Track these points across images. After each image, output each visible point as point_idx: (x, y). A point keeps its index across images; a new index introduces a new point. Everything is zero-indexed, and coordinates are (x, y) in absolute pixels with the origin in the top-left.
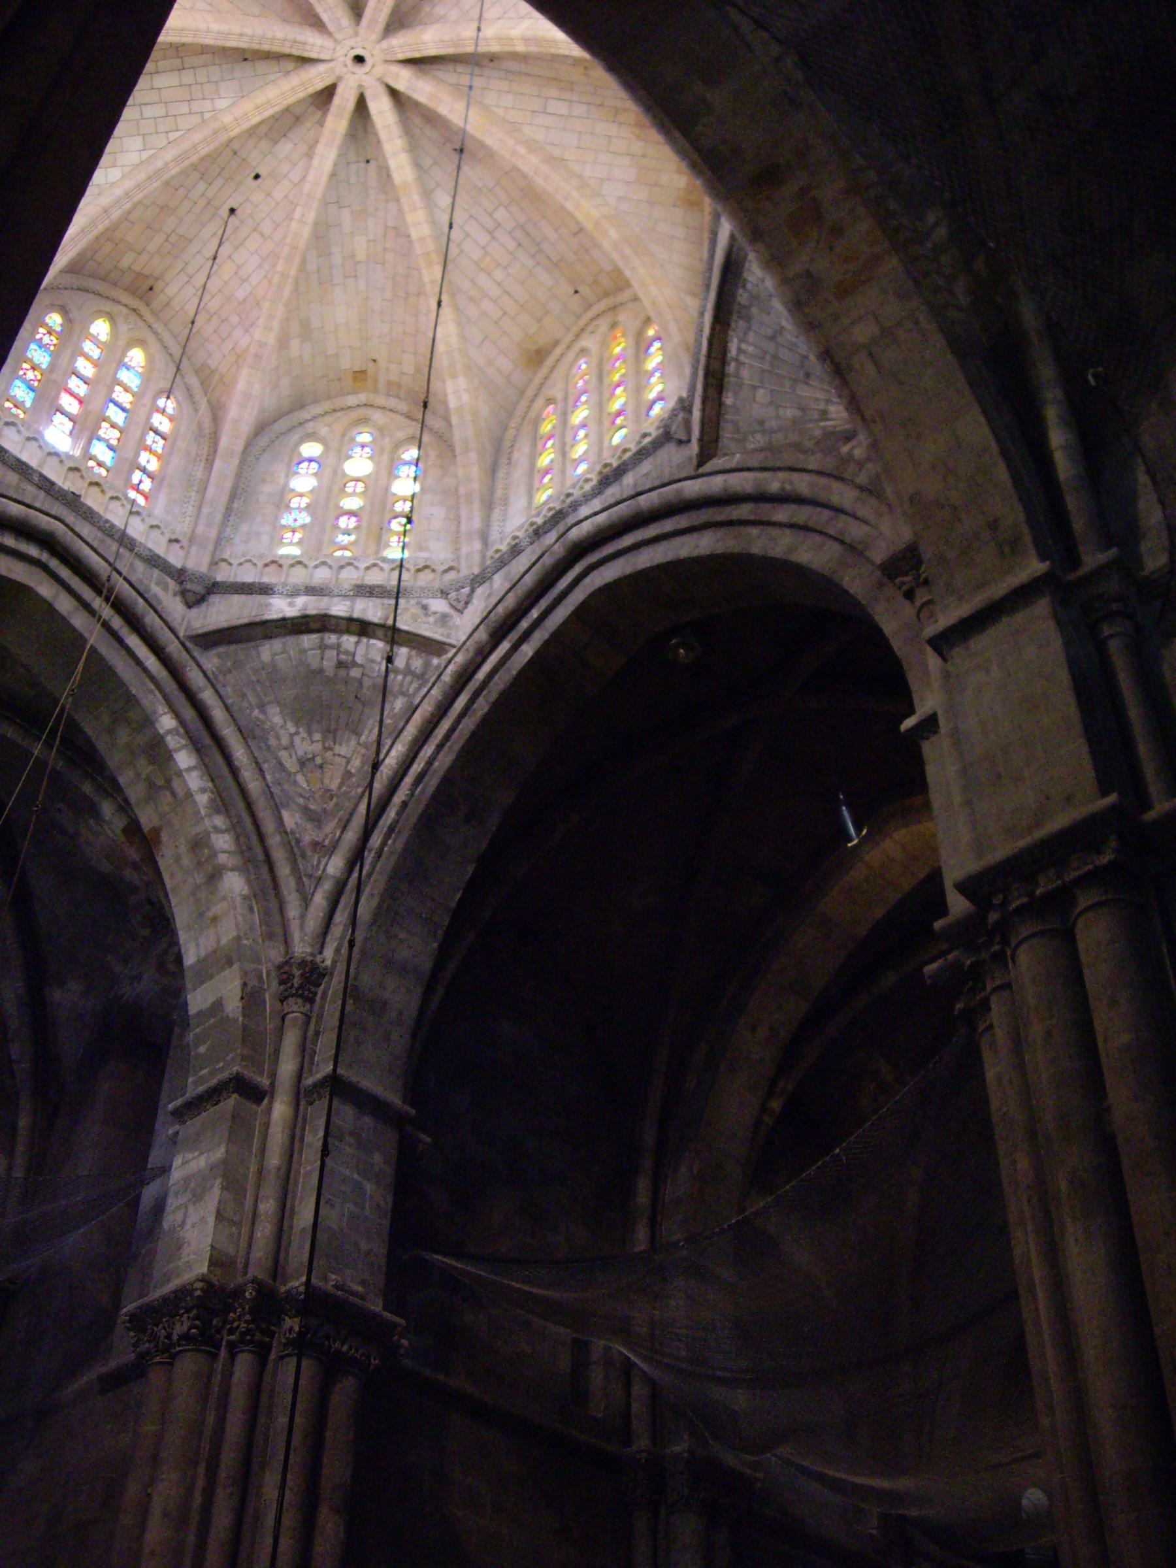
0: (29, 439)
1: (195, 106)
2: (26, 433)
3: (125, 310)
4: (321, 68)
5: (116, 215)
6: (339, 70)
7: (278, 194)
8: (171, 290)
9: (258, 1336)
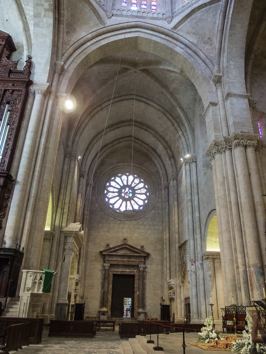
0: (128, 11)
2: (127, 10)
9: (228, 147)
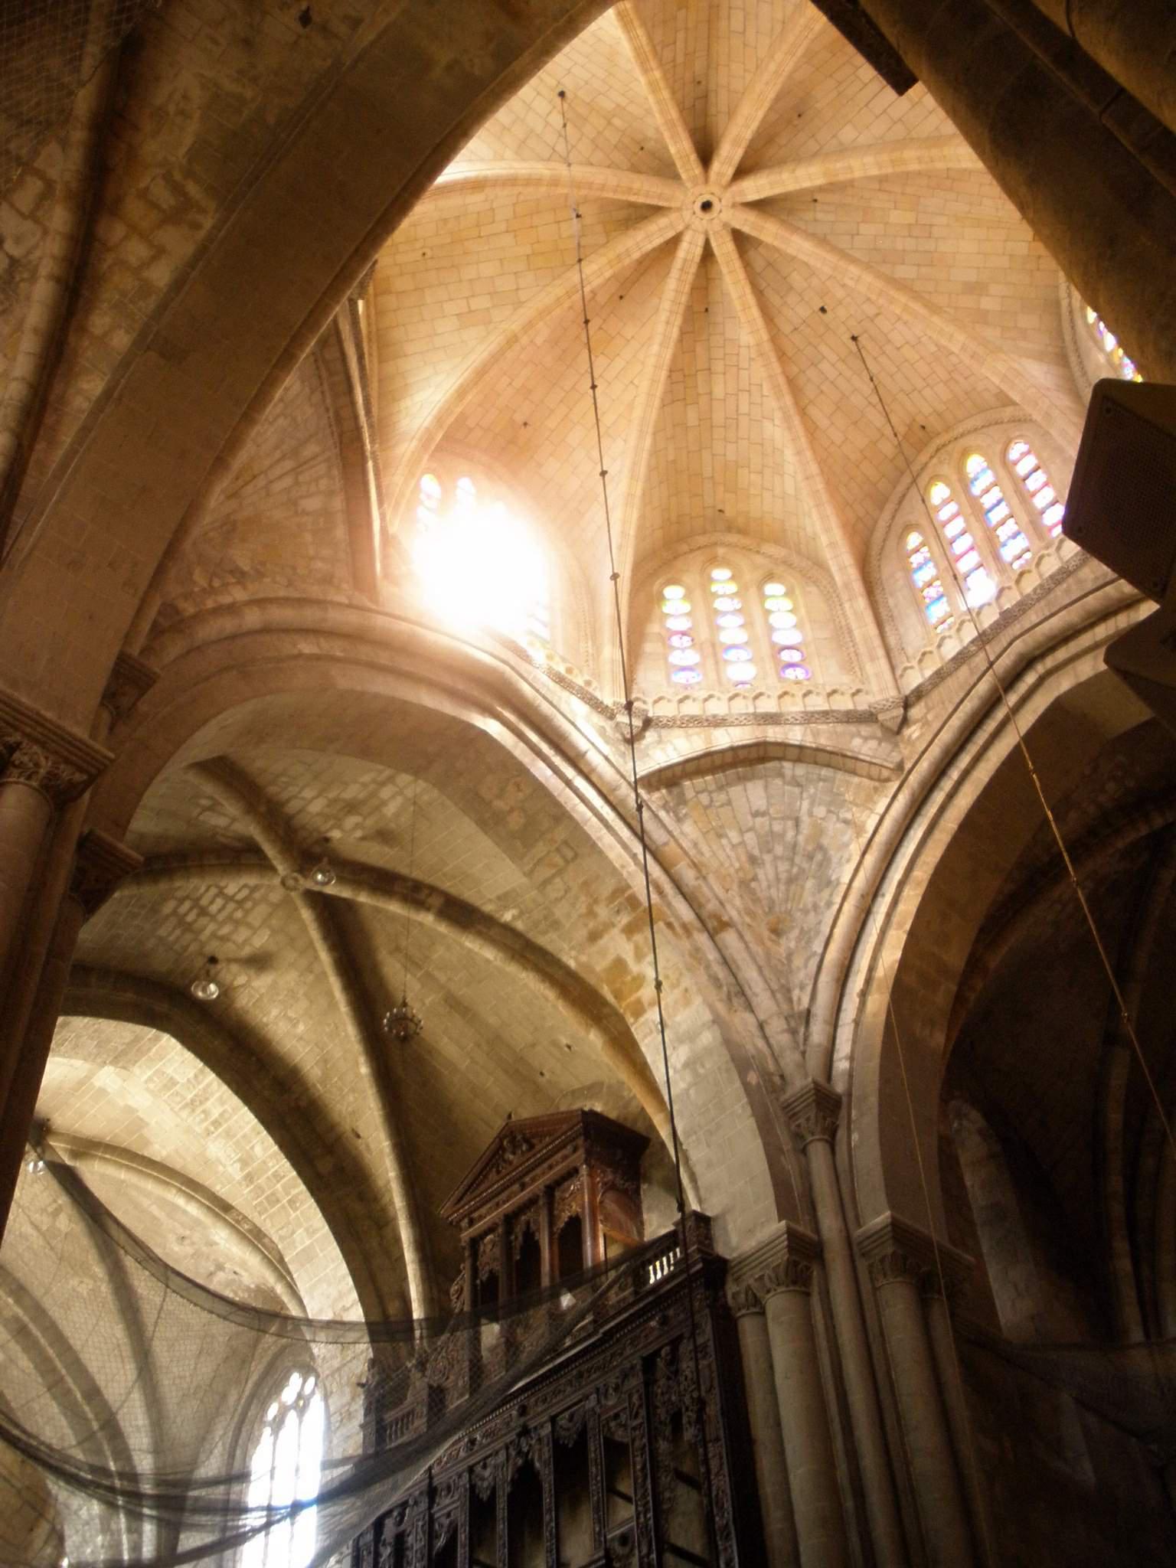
1: (744, 364)
3: (935, 460)
4: (714, 244)
5: (814, 468)
6: (717, 226)
7: (840, 294)
8: (927, 410)
